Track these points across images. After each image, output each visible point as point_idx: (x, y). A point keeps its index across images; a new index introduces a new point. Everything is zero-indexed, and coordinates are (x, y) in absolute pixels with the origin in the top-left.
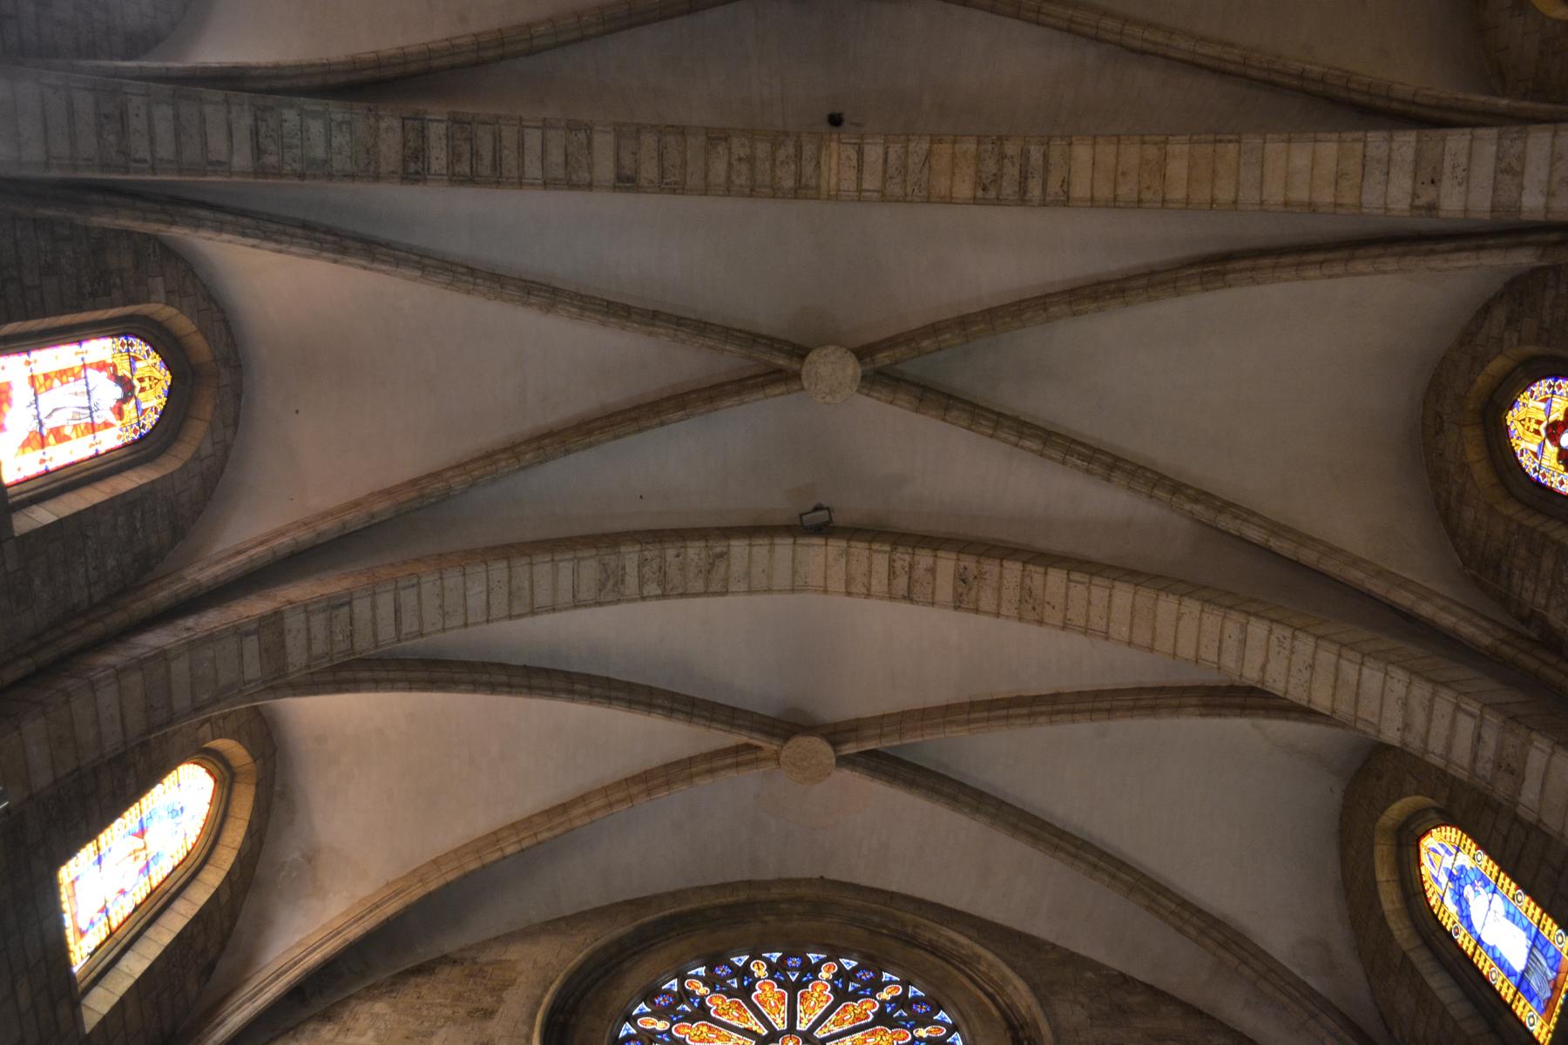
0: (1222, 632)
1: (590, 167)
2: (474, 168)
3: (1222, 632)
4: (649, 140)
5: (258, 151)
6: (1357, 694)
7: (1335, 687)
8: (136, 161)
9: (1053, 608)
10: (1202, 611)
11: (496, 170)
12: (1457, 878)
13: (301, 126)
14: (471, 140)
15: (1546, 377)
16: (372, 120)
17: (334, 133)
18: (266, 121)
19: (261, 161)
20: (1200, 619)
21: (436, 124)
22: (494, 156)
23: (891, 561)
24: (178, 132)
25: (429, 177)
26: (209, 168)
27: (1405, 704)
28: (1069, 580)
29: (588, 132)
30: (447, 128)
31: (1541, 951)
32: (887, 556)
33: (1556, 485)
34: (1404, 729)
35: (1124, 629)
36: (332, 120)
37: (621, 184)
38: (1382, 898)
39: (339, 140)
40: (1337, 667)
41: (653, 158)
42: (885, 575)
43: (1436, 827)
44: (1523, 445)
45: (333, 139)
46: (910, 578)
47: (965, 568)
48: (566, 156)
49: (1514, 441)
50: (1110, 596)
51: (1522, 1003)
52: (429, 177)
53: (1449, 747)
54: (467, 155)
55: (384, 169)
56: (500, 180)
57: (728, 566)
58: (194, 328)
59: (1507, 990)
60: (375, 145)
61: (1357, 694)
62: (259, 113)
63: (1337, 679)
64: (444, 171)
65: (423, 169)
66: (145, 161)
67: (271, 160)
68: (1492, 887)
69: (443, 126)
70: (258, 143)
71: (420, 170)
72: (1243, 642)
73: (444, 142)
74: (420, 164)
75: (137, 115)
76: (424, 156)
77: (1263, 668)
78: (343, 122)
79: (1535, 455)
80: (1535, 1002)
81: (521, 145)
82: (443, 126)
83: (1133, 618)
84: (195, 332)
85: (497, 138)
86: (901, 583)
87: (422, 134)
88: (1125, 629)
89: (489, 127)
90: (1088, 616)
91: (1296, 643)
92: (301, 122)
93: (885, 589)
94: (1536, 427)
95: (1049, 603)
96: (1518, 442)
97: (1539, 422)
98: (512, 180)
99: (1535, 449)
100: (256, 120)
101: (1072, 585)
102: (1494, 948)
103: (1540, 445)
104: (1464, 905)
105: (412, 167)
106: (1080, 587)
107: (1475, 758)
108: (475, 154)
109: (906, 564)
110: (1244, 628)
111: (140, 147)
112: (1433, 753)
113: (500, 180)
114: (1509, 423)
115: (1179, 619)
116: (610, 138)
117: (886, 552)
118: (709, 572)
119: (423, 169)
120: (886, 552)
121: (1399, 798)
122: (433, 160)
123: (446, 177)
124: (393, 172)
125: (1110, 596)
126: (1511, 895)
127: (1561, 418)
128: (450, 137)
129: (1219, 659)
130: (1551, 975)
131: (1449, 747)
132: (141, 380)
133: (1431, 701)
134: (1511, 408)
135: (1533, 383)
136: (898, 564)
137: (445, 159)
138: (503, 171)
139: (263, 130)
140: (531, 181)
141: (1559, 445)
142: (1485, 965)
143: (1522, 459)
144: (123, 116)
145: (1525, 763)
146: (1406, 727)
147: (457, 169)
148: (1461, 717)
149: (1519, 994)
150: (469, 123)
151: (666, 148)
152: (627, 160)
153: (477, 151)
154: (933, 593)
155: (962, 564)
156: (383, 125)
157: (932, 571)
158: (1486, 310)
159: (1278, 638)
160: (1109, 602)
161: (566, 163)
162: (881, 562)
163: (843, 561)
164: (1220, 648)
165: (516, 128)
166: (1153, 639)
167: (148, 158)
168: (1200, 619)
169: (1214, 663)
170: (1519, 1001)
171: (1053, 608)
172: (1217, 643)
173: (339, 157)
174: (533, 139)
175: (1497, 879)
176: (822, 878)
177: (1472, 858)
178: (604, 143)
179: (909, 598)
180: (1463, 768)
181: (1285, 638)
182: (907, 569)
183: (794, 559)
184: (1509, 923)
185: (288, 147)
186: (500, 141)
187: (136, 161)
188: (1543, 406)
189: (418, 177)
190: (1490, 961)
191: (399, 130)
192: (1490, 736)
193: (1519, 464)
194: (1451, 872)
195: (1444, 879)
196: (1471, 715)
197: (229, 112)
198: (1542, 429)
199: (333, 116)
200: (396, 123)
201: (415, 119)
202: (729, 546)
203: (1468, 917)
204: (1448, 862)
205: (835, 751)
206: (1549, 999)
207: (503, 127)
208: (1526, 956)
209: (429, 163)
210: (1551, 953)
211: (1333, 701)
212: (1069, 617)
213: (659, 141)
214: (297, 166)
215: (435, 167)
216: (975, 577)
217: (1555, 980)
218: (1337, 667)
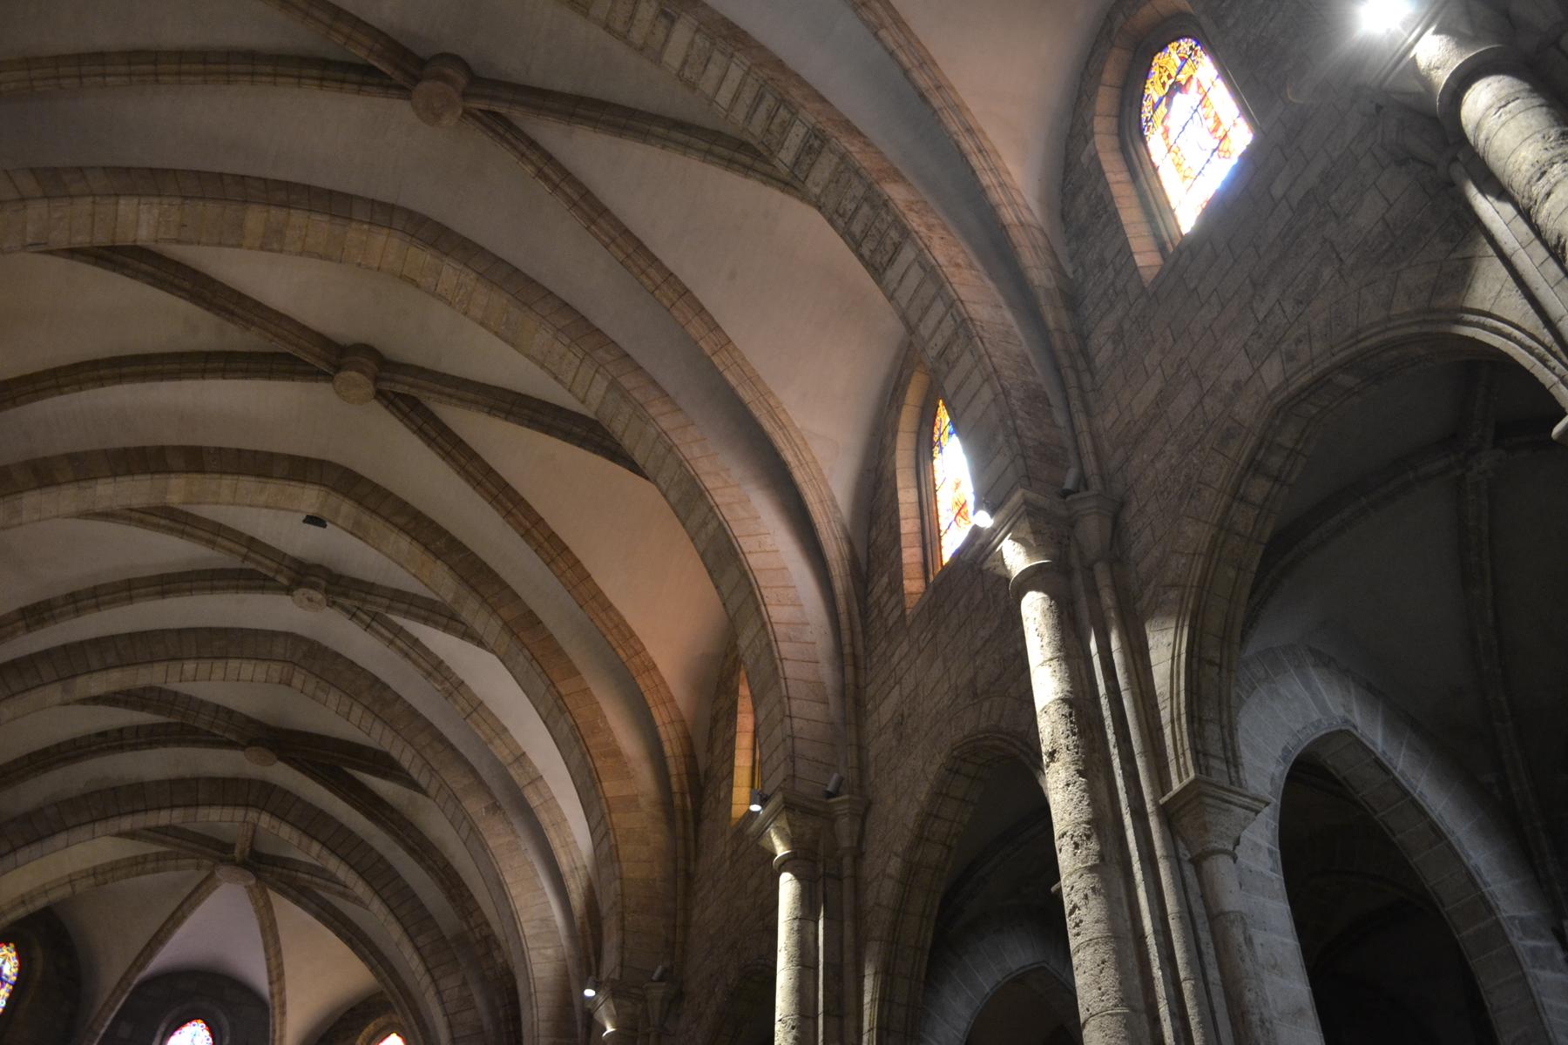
1: (692, 43)
2: (776, 108)
4: (637, 36)
5: (897, 248)
8: (955, 321)
11: (762, 94)
13: (864, 238)
14: (768, 130)
16: (822, 200)
17: (850, 213)
18: (881, 263)
19: (900, 240)
21: (785, 161)
22: (758, 105)
24: (926, 310)
25: (811, 127)
26: (928, 270)
29: (681, 74)
30: (779, 152)
36: (846, 223)
37: (673, 14)
39: (851, 206)
41: (639, 20)
45: (853, 210)
48: (706, 65)
52: (811, 127)
54: (777, 121)
55: (836, 160)
56: (763, 83)
58: (1102, 90)
60: (831, 181)
62: (881, 271)
64: (798, 122)
65: (810, 136)
66: (952, 315)
67: (894, 234)
69: (780, 156)
70: (894, 254)
71: (813, 137)
73: (786, 144)
74: (811, 142)
75: (936, 345)
76: (805, 144)
78: (840, 216)
81: (736, 98)
82: (780, 156)
84: (1104, 85)
85: (749, 117)
87: (797, 162)
89: (751, 130)
92: (862, 240)
98: (756, 77)
100: (885, 269)
105: (817, 144)
108: (771, 117)
111: (948, 326)
113: (763, 83)
116: (666, 58)
119: (810, 136)
122: (801, 136)
123: (800, 117)
124: (831, 152)
128: (781, 144)
132: (1164, 84)
137: (792, 131)
138: (757, 88)
139: (886, 259)
140: (742, 65)
144: (942, 354)
147: (788, 116)
150: (762, 142)
151: (626, 22)
152: (660, 34)
153: (768, 119)
156: (817, 190)
161: (708, 60)
165: (732, 114)
167: (949, 314)
173: (857, 195)
174: (724, 97)
178: (673, 58)
185: (880, 232)
186: (748, 113)
187: (955, 321)
189: (817, 133)
191: (811, 178)
197: (895, 290)
199: (843, 225)
200: (809, 184)
201: (796, 176)
207: (741, 122)
209: (804, 138)
213: (629, 31)
214: (883, 213)
215: (802, 131)
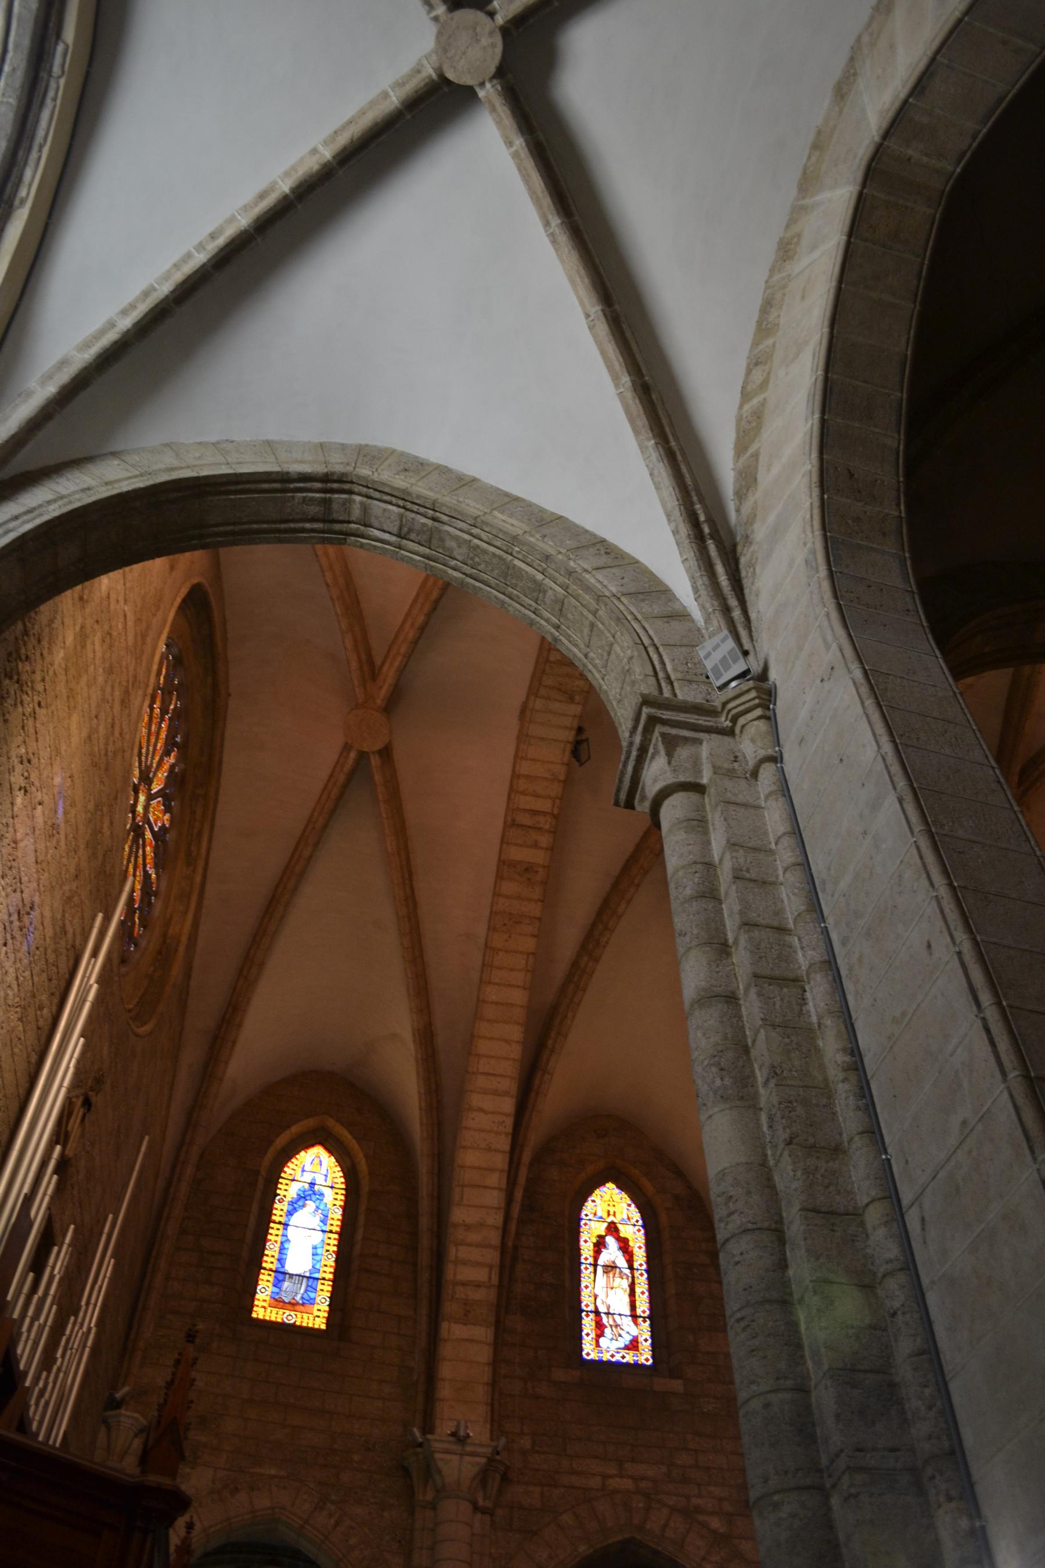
0: (501, 1076)
3: (501, 1076)
6: (479, 1186)
7: (479, 1168)
9: (506, 941)
10: (514, 1060)
12: (311, 1192)
15: (643, 1218)
20: (507, 1059)
23: (545, 814)
27: (481, 1225)
28: (528, 954)
31: (308, 1286)
32: (549, 810)
33: (584, 1237)
34: (466, 1226)
35: (494, 997)
38: (283, 1135)
40: (492, 1170)
42: (533, 807)
43: (337, 1161)
44: (598, 1201)
46: (530, 827)
47: (537, 872)
49: (597, 1192)
50: (518, 987)
51: (269, 1278)
53: (465, 1263)
57: (560, 701)
59: (269, 1261)
61: (479, 1186)
63: (485, 1169)
68: (324, 1228)
72: (496, 1093)
77: (480, 1110)
79: (595, 1214)
80: (276, 1290)
83: (502, 1004)
86: (525, 819)
88: (494, 998)
90: (501, 968)
91: (503, 1136)
93: (522, 806)
94: (612, 1213)
95: (510, 937)
96: (599, 1196)
97: (614, 1215)
99: (599, 1214)
101: (525, 957)
102: (288, 1240)
103: (601, 1218)
104: (300, 1203)
106: (524, 962)
107: (464, 1284)
109: (541, 826)
110: (506, 1094)
112: (457, 1251)
114: (608, 1185)
115: (507, 1041)
117: (552, 810)
118: (560, 690)
120: (552, 810)
121: (355, 1138)
125: (518, 987)
126: (328, 1247)
127: (622, 1235)
129: (481, 1073)
130: (298, 1298)
131: (465, 1263)
133: (489, 1246)
134: (618, 1187)
135: (637, 1207)
136: (542, 819)
141: (606, 1235)
142: (274, 1233)
143: (590, 1202)
145: (474, 1324)
146: (468, 1227)
148: (486, 1270)
149: (273, 1274)
154: (516, 845)
155: (540, 869)
157: (536, 845)
158: (680, 1173)
159: (503, 1122)
160: (514, 986)
162: (545, 805)
163: (547, 775)
164: (488, 1074)
166: (489, 1021)
168: (507, 1059)
169: (478, 1068)
170: (269, 1275)
171: (506, 941)
172: (491, 1071)
175: (331, 1232)
176: (229, 695)
177: (333, 1200)
179: (511, 824)
180: (455, 1275)
181: (505, 1127)
182: (538, 825)
183: (555, 740)
184: (311, 1251)
188: (625, 1217)
190: (279, 1239)
192: (479, 1295)
193: (586, 1200)
194: (315, 1184)
195: (308, 1178)
196: (490, 1278)
198: (610, 1219)
202: (579, 703)
203: (295, 1210)
204: (320, 1180)
205: (373, 753)
206: (284, 1302)
208: (298, 1273)
210: (312, 1295)
211: (470, 1167)
212: (500, 953)
216: (529, 879)
217: (297, 1304)
218: (492, 1170)
